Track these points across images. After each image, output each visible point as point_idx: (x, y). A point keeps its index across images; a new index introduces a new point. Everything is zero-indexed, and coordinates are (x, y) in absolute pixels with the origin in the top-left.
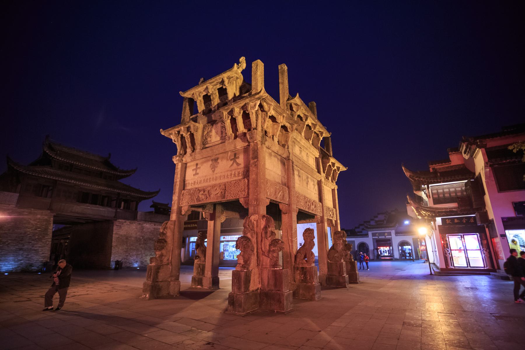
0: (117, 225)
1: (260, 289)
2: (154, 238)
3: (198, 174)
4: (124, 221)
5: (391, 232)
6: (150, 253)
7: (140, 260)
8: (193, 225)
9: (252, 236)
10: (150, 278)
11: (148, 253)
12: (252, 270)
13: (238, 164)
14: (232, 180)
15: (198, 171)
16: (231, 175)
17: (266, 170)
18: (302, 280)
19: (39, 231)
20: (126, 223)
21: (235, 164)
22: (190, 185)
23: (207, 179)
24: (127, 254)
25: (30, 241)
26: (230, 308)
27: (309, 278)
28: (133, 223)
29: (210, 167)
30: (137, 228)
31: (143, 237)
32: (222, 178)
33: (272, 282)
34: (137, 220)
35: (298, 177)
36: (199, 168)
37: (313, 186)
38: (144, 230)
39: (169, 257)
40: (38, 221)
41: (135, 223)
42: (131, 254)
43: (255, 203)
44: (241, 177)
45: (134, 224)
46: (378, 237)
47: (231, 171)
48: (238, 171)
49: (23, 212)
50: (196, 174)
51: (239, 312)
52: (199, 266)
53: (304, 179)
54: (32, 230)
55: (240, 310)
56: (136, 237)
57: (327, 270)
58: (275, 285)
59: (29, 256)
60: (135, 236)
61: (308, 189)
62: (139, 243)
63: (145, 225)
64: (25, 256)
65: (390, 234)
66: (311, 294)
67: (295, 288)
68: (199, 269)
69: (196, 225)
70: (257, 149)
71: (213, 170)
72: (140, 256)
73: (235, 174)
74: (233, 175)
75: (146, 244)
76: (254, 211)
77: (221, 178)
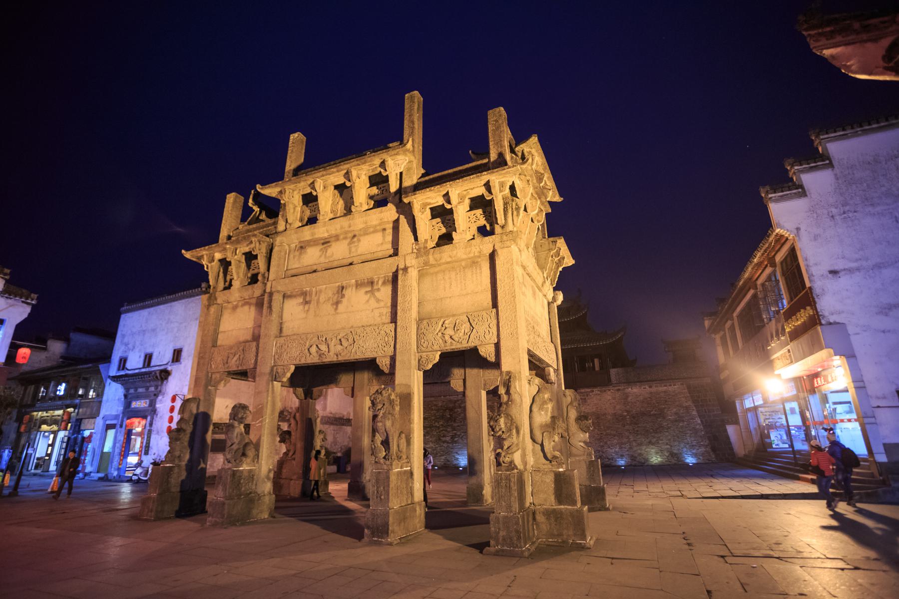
4: (589, 390)
6: (648, 441)
7: (627, 453)
11: (643, 440)
20: (594, 393)
24: (601, 444)
28: (605, 391)
30: (614, 398)
34: (611, 385)
35: (301, 307)
38: (629, 399)
41: (610, 390)
42: (609, 443)
45: (609, 393)
60: (613, 412)
62: (621, 423)
63: (630, 389)
72: (627, 446)
75: (636, 424)
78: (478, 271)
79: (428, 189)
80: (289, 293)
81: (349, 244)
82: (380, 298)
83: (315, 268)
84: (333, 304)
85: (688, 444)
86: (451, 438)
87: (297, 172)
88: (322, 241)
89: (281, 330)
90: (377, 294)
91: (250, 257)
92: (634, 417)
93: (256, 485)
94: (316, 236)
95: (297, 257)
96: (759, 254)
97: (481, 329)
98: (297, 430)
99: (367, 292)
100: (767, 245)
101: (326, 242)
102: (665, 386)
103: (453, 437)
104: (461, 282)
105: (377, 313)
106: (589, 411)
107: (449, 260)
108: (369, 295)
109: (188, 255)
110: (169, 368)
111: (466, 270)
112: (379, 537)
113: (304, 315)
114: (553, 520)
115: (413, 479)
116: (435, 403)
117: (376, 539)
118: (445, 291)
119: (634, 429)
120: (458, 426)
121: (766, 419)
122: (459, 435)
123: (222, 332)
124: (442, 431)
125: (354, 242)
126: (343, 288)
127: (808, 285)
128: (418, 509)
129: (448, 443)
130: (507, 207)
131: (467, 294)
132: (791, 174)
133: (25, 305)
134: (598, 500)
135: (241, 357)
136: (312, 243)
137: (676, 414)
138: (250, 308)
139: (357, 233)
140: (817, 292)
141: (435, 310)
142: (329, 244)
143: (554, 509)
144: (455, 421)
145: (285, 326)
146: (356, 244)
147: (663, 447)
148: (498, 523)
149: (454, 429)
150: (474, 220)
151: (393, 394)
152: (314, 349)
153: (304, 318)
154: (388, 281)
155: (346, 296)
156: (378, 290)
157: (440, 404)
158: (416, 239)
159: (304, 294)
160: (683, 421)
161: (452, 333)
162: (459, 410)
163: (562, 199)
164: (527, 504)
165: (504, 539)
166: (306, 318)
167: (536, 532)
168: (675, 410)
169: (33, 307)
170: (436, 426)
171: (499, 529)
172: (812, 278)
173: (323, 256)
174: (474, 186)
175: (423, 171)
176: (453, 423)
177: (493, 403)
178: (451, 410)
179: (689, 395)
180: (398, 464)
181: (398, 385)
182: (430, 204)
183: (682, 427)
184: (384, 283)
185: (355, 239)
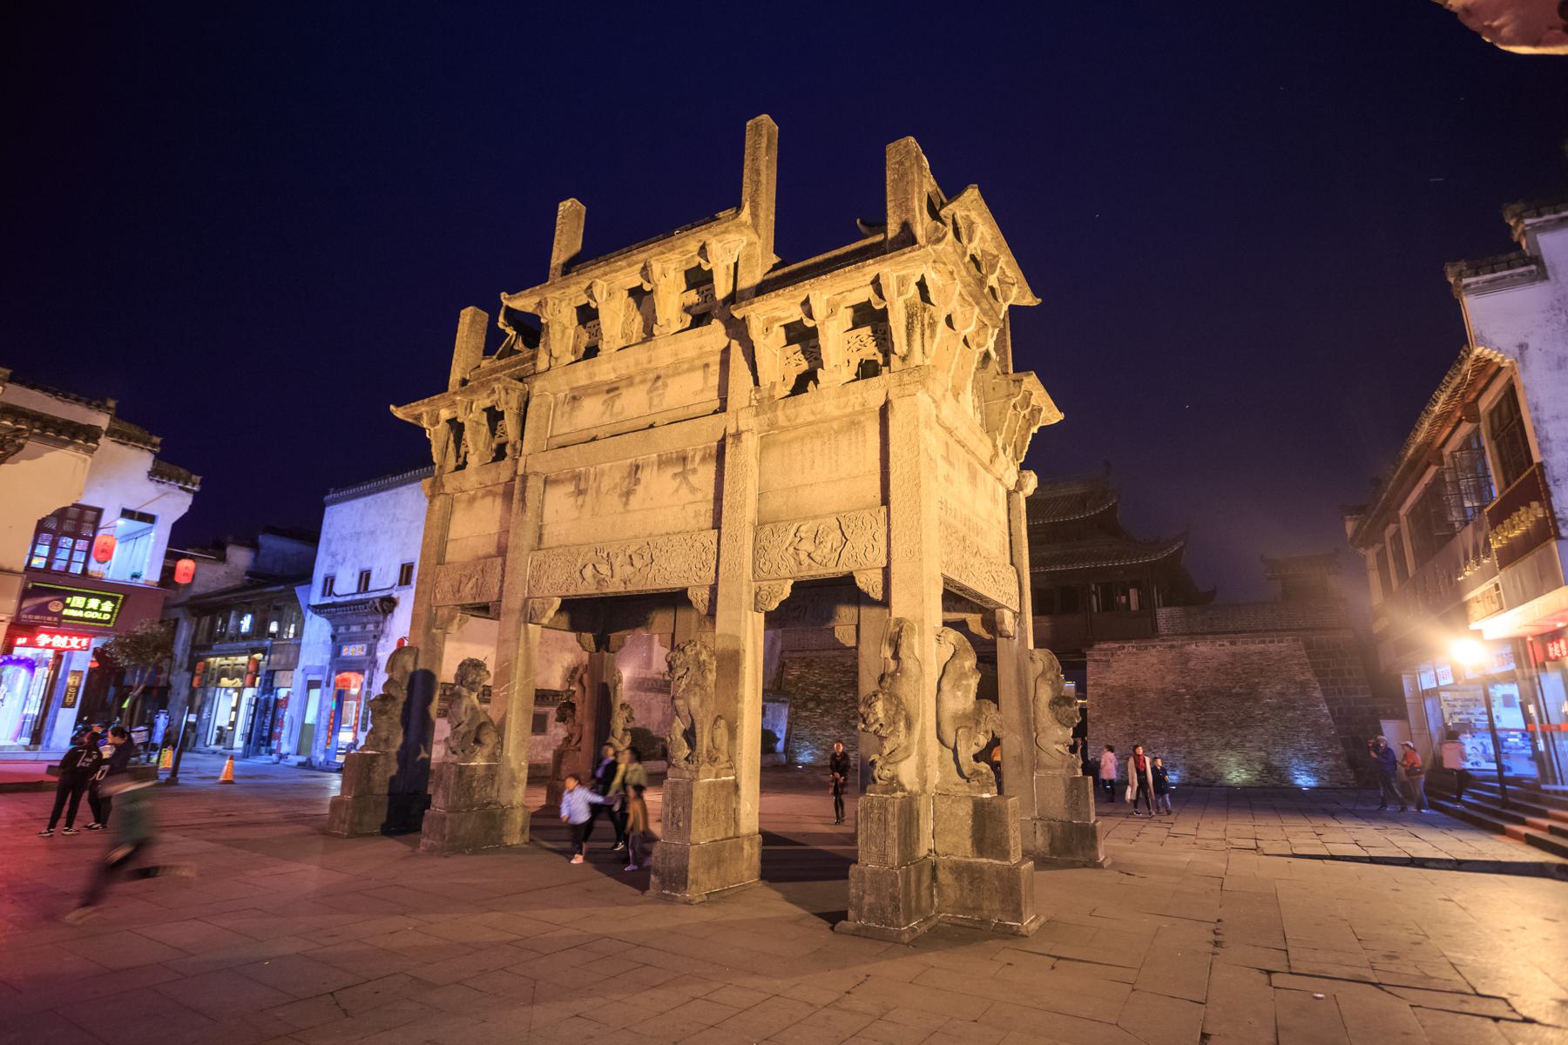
0: (1095, 661)
2: (1235, 687)
4: (1117, 645)
6: (1223, 741)
7: (1183, 761)
11: (1215, 739)
28: (1146, 648)
30: (1162, 662)
34: (1158, 637)
35: (572, 500)
38: (1191, 664)
41: (1154, 647)
42: (1148, 741)
45: (1153, 651)
56: (1163, 691)
60: (1160, 687)
62: (1174, 707)
63: (1194, 646)
72: (1184, 749)
75: (1201, 709)
78: (860, 439)
79: (773, 294)
80: (553, 476)
81: (650, 391)
82: (696, 486)
83: (594, 433)
84: (620, 496)
85: (1301, 750)
87: (569, 267)
88: (607, 388)
89: (540, 537)
90: (692, 478)
91: (494, 416)
92: (1198, 698)
93: (498, 791)
94: (597, 379)
95: (566, 416)
96: (1443, 397)
97: (859, 542)
98: (584, 702)
99: (675, 475)
100: (1458, 380)
101: (612, 389)
102: (1264, 642)
104: (830, 458)
105: (690, 510)
106: (1115, 684)
107: (811, 418)
108: (678, 480)
109: (399, 412)
110: (395, 595)
111: (840, 437)
112: (672, 889)
113: (576, 514)
114: (966, 883)
115: (739, 797)
116: (839, 659)
117: (667, 892)
118: (803, 473)
119: (1197, 719)
121: (1455, 713)
123: (453, 540)
124: (851, 708)
125: (657, 389)
126: (637, 467)
127: (1537, 458)
128: (746, 846)
130: (913, 322)
131: (841, 479)
132: (1516, 235)
133: (184, 493)
134: (1083, 848)
135: (480, 582)
136: (589, 391)
137: (1281, 694)
138: (494, 501)
139: (662, 373)
140: (1555, 474)
141: (784, 508)
142: (617, 392)
143: (969, 863)
145: (546, 532)
146: (660, 392)
147: (1252, 754)
148: (863, 881)
150: (857, 346)
151: (704, 652)
152: (589, 572)
153: (574, 520)
154: (710, 455)
155: (642, 481)
156: (694, 471)
157: (850, 663)
158: (756, 382)
159: (577, 478)
160: (1294, 709)
161: (811, 548)
163: (1039, 300)
164: (923, 852)
165: (871, 910)
166: (578, 518)
167: (936, 900)
168: (1279, 687)
169: (196, 496)
170: (841, 700)
171: (864, 892)
172: (1547, 445)
173: (608, 413)
174: (852, 286)
175: (775, 259)
179: (1307, 660)
180: (710, 771)
181: (720, 635)
182: (779, 319)
183: (1291, 719)
184: (703, 460)
185: (660, 383)
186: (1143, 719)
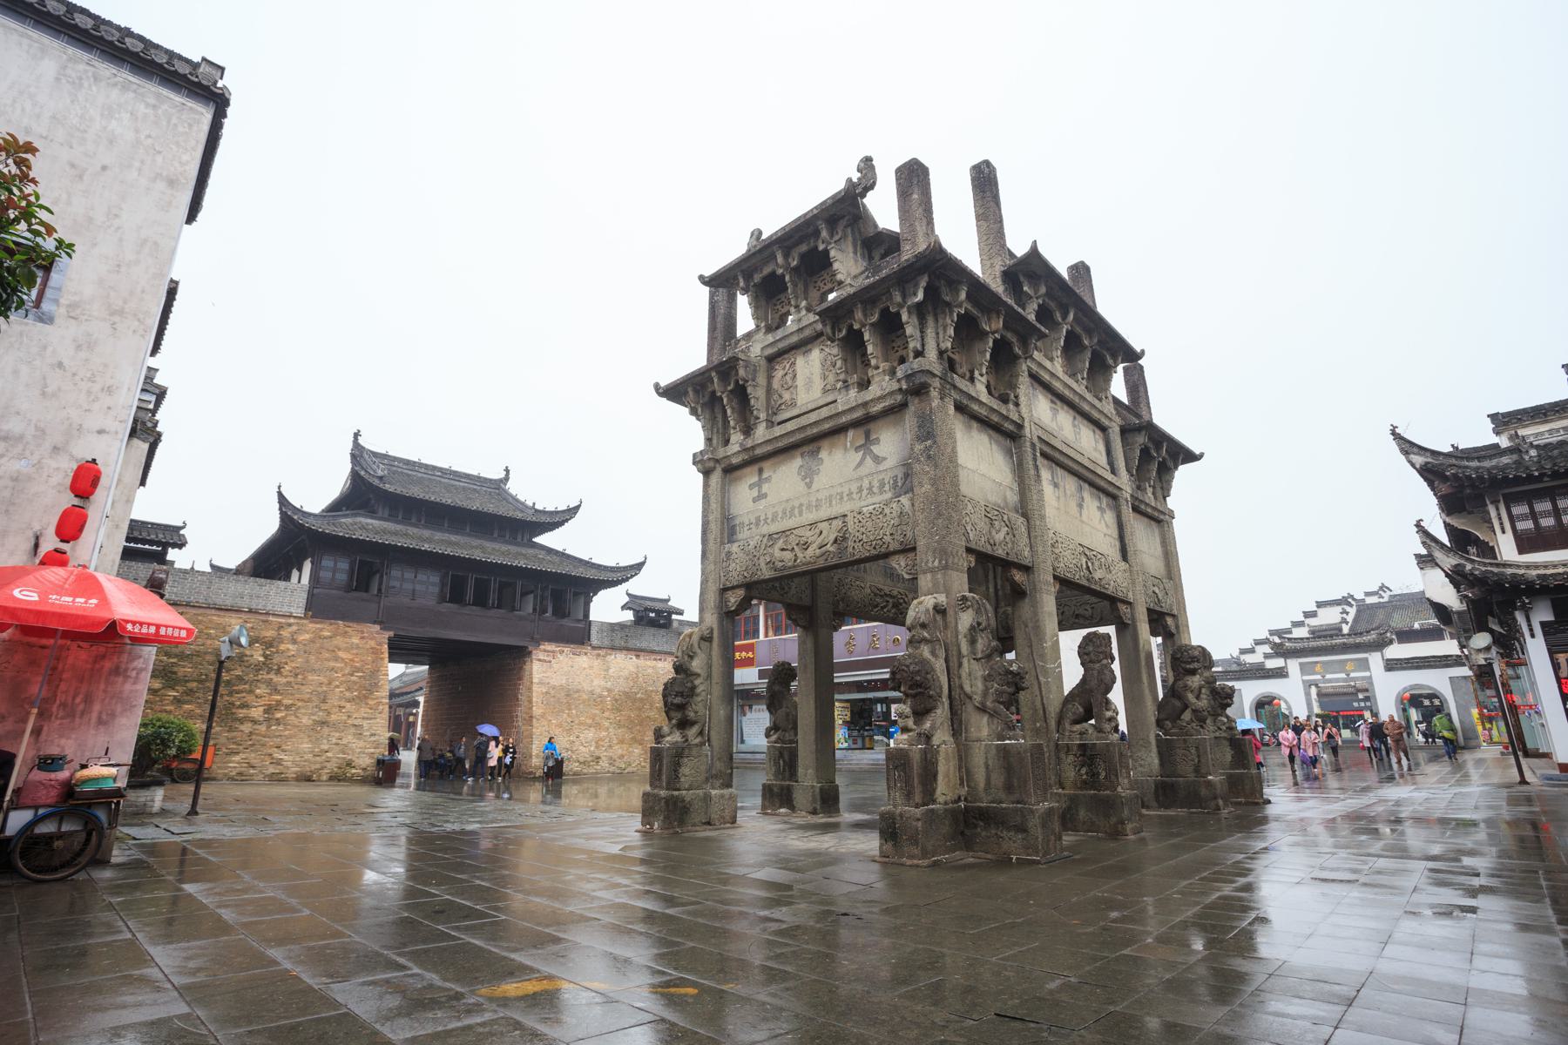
0: (540, 660)
1: (966, 799)
3: (765, 496)
5: (1367, 659)
8: (744, 654)
9: (933, 653)
10: (660, 779)
12: (938, 746)
13: (878, 460)
14: (863, 503)
15: (765, 488)
16: (860, 490)
17: (960, 469)
18: (1085, 782)
19: (360, 677)
21: (869, 460)
22: (746, 529)
23: (793, 508)
25: (343, 704)
26: (889, 847)
27: (1104, 774)
29: (799, 474)
31: (609, 690)
32: (834, 502)
33: (998, 779)
35: (1052, 487)
36: (768, 479)
37: (1098, 514)
38: (611, 671)
39: (704, 725)
40: (355, 651)
41: (586, 654)
43: (936, 563)
44: (889, 495)
46: (1323, 677)
47: (861, 478)
48: (881, 477)
49: (321, 630)
50: (761, 496)
51: (912, 857)
52: (781, 755)
53: (1068, 492)
54: (343, 675)
55: (916, 852)
56: (592, 693)
57: (1156, 761)
58: (1009, 788)
59: (344, 741)
61: (1083, 522)
64: (334, 741)
65: (1364, 665)
66: (1113, 820)
67: (1064, 806)
68: (781, 762)
69: (750, 655)
70: (931, 412)
71: (808, 480)
73: (870, 489)
74: (865, 492)
76: (934, 585)
77: (831, 501)
86: (266, 712)
92: (616, 700)
102: (655, 659)
103: (269, 710)
120: (289, 683)
122: (288, 707)
129: (255, 722)
144: (278, 672)
149: (276, 691)
162: (290, 647)
176: (272, 676)
177: (380, 644)
178: (269, 644)
186: (577, 716)
